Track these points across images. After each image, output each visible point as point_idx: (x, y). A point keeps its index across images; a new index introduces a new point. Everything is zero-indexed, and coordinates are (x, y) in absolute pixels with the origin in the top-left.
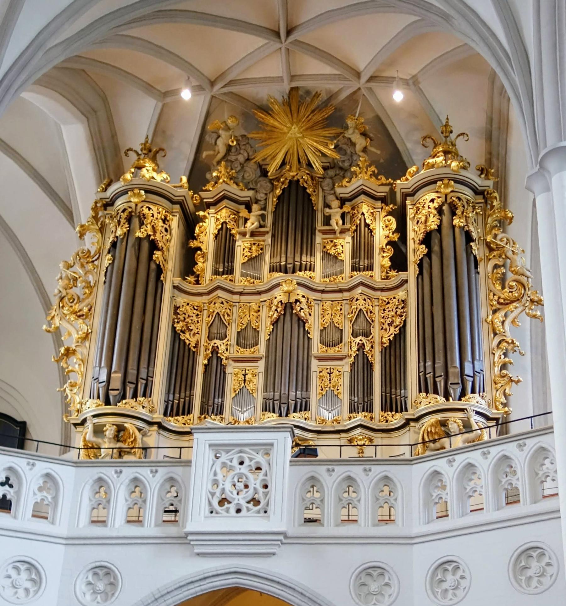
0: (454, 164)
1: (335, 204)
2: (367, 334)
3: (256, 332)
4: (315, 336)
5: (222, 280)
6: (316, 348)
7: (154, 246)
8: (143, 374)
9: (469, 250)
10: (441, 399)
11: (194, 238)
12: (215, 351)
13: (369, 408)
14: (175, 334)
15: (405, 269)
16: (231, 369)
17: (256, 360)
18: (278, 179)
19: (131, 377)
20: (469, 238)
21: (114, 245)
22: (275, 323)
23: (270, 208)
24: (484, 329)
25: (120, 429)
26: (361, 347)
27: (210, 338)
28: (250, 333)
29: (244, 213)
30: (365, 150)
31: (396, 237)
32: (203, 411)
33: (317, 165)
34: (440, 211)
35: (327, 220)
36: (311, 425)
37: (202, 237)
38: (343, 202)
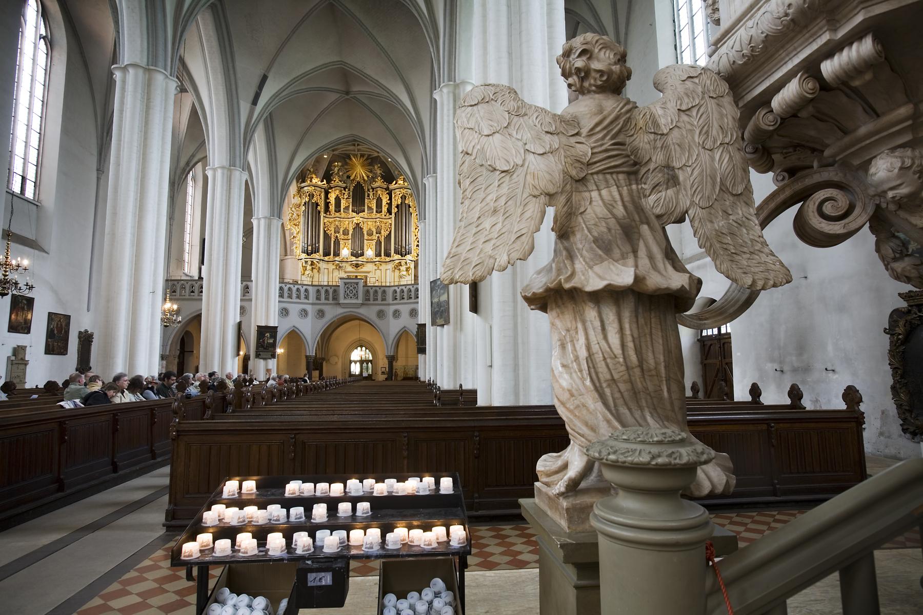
0: (406, 184)
1: (371, 190)
2: (380, 233)
3: (348, 231)
4: (365, 233)
5: (337, 214)
6: (366, 237)
7: (317, 205)
8: (317, 245)
9: (409, 211)
10: (400, 256)
11: (328, 199)
12: (337, 237)
13: (380, 256)
14: (325, 231)
15: (391, 214)
16: (342, 242)
17: (348, 240)
18: (353, 180)
19: (314, 246)
20: (409, 207)
21: (305, 203)
22: (354, 229)
23: (351, 190)
24: (413, 235)
25: (312, 262)
26: (378, 237)
27: (335, 233)
28: (346, 231)
29: (344, 192)
30: (380, 173)
31: (389, 202)
32: (334, 255)
33: (366, 178)
34: (401, 198)
35: (368, 196)
36: (365, 260)
37: (331, 199)
38: (373, 189)
